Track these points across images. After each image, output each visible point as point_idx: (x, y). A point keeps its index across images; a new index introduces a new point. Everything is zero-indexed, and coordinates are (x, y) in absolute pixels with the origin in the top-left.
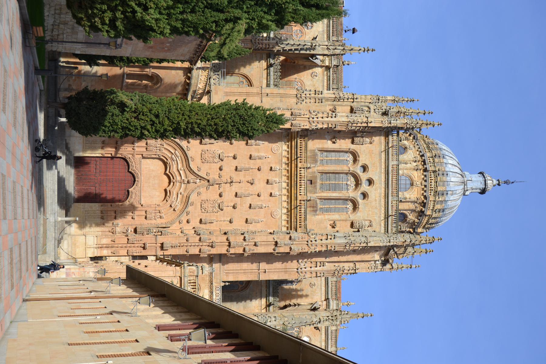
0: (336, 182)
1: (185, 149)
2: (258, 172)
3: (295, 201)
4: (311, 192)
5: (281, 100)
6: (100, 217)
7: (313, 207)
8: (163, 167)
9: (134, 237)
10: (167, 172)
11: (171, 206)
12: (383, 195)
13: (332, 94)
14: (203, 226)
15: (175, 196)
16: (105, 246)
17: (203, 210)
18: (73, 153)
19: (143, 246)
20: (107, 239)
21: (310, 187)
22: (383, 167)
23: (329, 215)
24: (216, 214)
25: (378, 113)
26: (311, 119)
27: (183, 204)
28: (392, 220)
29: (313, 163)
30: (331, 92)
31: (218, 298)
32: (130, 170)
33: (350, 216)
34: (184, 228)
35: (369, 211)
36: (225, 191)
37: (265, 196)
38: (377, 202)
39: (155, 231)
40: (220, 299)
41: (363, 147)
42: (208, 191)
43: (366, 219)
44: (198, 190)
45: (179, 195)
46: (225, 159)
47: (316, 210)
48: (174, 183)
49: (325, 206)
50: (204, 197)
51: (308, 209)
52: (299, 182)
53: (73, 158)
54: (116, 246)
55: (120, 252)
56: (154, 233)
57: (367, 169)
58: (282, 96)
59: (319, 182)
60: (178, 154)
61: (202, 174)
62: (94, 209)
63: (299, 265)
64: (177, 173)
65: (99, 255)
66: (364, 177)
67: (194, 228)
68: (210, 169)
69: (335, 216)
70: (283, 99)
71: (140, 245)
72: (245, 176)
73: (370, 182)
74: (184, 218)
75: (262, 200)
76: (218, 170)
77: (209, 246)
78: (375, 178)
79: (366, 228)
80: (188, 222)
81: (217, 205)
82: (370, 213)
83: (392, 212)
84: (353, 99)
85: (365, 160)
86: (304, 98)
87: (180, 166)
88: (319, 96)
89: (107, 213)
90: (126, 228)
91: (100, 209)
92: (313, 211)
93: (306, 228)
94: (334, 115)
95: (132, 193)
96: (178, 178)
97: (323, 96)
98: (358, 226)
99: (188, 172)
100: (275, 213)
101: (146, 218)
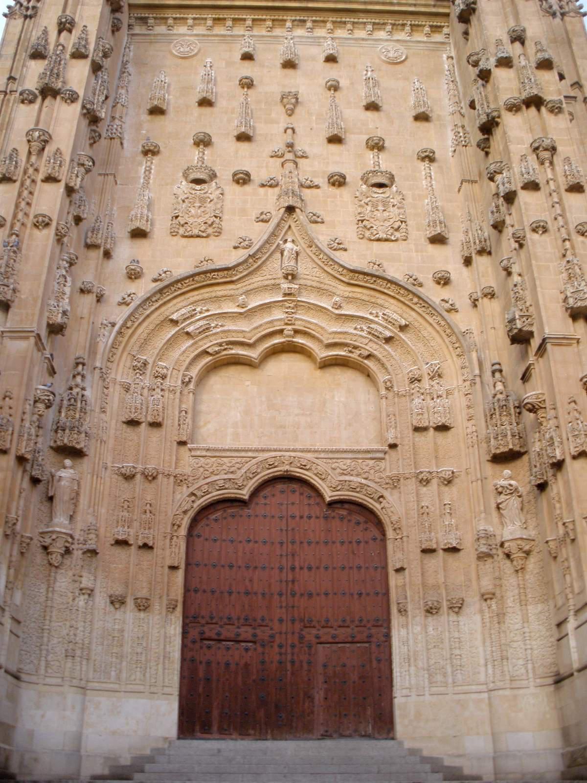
6: (453, 617)
8: (232, 372)
10: (254, 354)
11: (388, 340)
14: (456, 237)
15: (349, 328)
17: (398, 235)
24: (409, 200)
27: (381, 299)
32: (245, 494)
39: (500, 386)
42: (326, 219)
45: (343, 312)
48: (297, 332)
50: (348, 233)
61: (258, 233)
64: (259, 321)
68: (243, 212)
74: (434, 294)
75: (352, 84)
76: (247, 188)
81: (379, 194)
87: (230, 308)
89: (436, 587)
91: (420, 618)
96: (278, 314)
99: (256, 280)
101: (443, 428)
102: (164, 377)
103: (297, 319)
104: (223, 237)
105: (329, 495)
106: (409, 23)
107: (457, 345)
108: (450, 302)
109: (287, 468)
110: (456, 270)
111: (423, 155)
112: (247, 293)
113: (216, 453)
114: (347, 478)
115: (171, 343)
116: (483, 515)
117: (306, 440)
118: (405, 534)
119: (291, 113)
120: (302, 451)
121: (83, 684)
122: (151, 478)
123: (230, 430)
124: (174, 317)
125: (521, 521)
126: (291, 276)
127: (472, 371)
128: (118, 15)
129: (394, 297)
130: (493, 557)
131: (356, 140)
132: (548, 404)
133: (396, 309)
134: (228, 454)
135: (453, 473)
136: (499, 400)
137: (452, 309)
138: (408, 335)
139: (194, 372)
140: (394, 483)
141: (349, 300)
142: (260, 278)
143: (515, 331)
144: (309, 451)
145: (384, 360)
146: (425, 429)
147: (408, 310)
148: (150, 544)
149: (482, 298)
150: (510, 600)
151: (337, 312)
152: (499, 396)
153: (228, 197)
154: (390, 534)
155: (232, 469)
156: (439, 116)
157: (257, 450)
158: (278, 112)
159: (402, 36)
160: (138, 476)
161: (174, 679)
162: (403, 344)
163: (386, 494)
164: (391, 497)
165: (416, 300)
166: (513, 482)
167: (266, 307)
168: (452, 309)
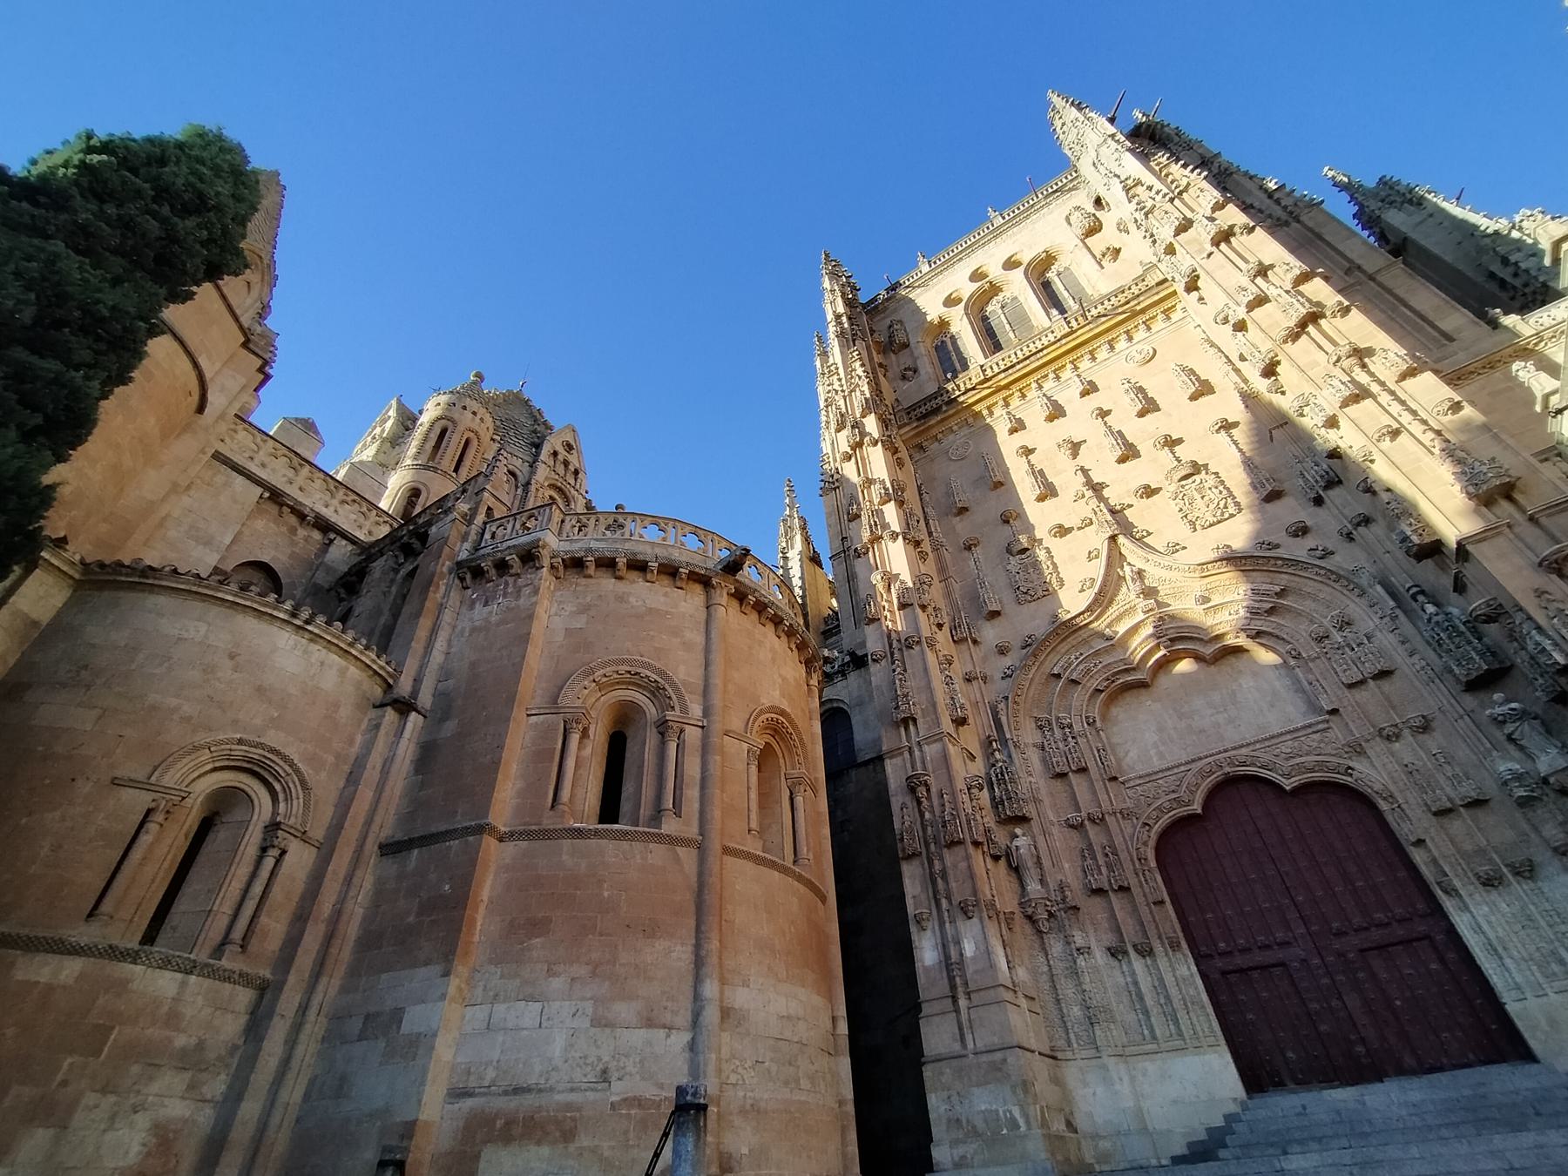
8: (1129, 698)
11: (1271, 611)
18: (1233, 1108)
32: (1197, 807)
37: (1094, 401)
39: (1430, 608)
74: (1298, 549)
100: (1138, 357)
101: (1384, 674)
102: (1070, 726)
103: (1166, 629)
105: (1288, 784)
106: (1140, 322)
107: (1351, 587)
108: (1320, 548)
109: (1227, 769)
110: (1307, 515)
111: (1217, 427)
113: (1149, 777)
114: (1298, 760)
116: (1495, 753)
117: (1232, 736)
118: (1401, 801)
120: (1234, 748)
121: (1120, 1050)
122: (1098, 820)
123: (1153, 752)
125: (1556, 747)
128: (899, 455)
129: (1253, 570)
130: (1541, 800)
132: (1508, 607)
133: (1263, 580)
134: (1161, 775)
135: (1423, 717)
136: (1437, 623)
137: (1327, 553)
138: (1290, 598)
139: (1096, 713)
140: (1358, 750)
142: (1115, 608)
143: (1415, 548)
144: (1242, 746)
145: (1276, 632)
146: (1362, 682)
147: (1277, 575)
148: (1126, 884)
149: (1355, 529)
152: (1435, 619)
154: (1384, 806)
155: (1173, 788)
157: (1187, 763)
160: (1086, 822)
162: (1288, 609)
164: (1359, 765)
165: (1280, 562)
166: (1513, 705)
168: (1327, 553)
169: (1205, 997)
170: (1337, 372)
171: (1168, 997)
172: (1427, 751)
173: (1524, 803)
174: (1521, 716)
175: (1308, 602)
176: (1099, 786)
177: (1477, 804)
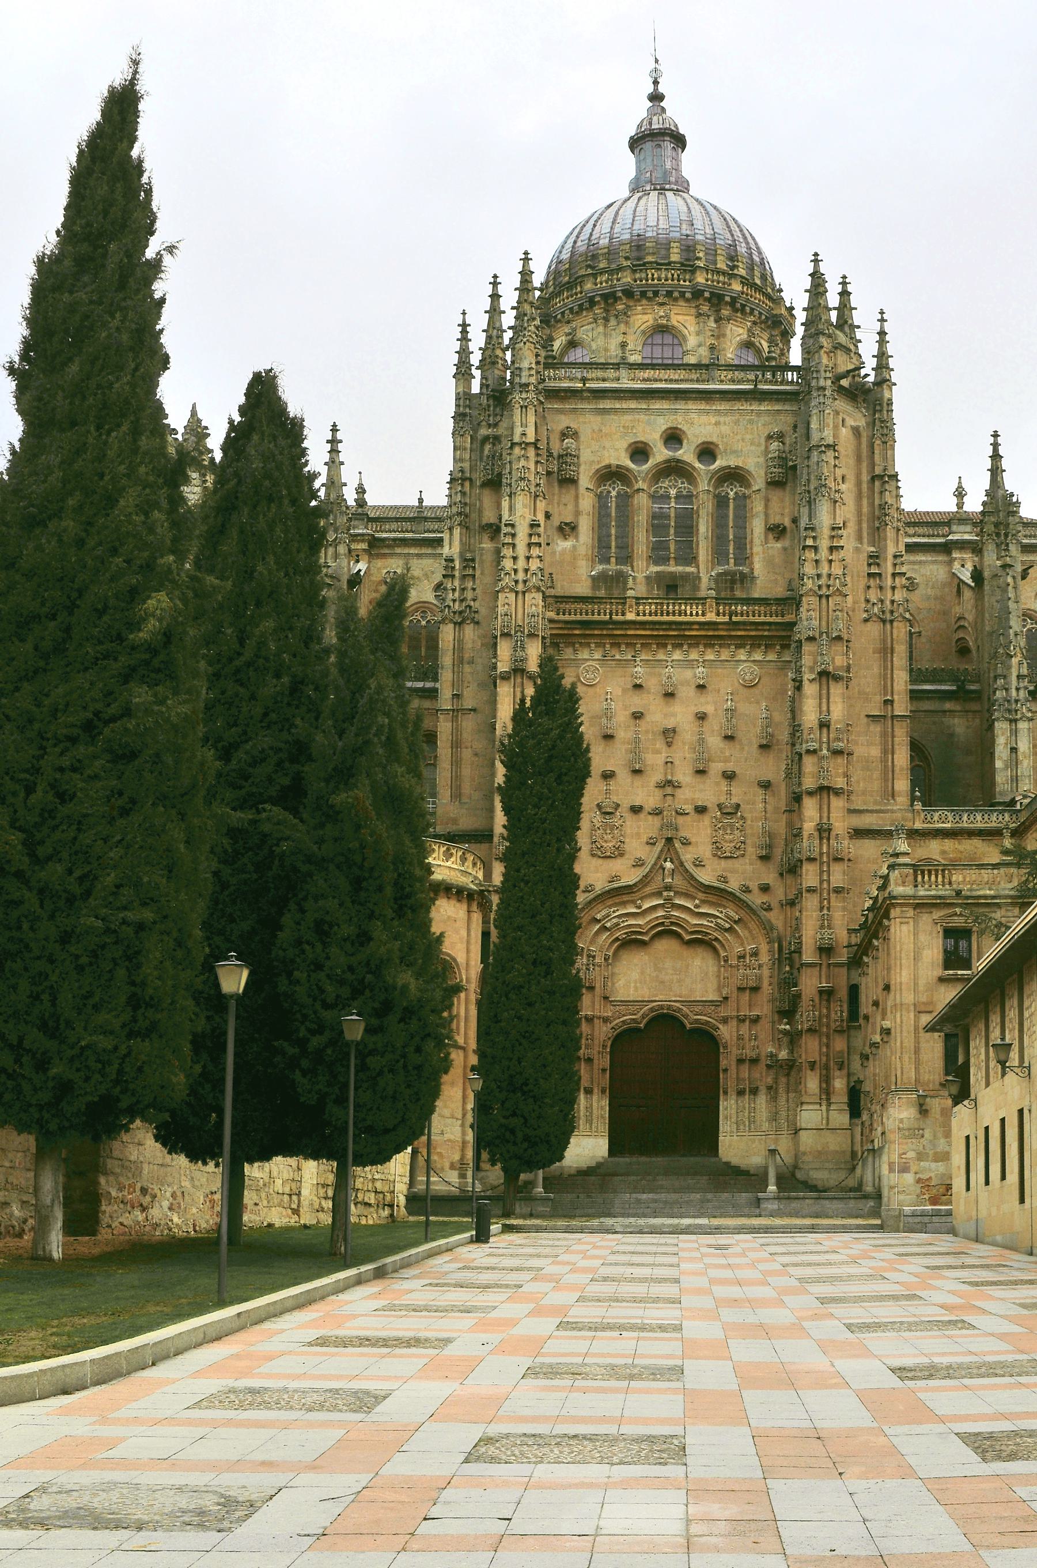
0: (673, 524)
1: (591, 896)
2: (648, 718)
3: (720, 627)
4: (696, 588)
5: (468, 663)
7: (733, 582)
9: (804, 1017)
10: (646, 938)
11: (726, 930)
12: (703, 406)
13: (451, 534)
14: (778, 852)
16: (824, 1085)
18: (601, 1160)
19: (825, 997)
20: (809, 1079)
21: (684, 591)
22: (633, 404)
23: (752, 542)
24: (749, 822)
25: (499, 418)
26: (520, 587)
27: (724, 902)
28: (766, 382)
29: (625, 583)
30: (446, 536)
31: (950, 818)
33: (756, 488)
34: (783, 898)
35: (743, 440)
36: (693, 799)
38: (722, 419)
39: (788, 968)
40: (953, 811)
41: (586, 455)
42: (693, 840)
43: (763, 448)
44: (689, 866)
46: (615, 799)
47: (743, 577)
48: (672, 923)
49: (731, 551)
51: (738, 594)
52: (671, 618)
53: (612, 1159)
54: (824, 1059)
55: (838, 1049)
56: (795, 972)
57: (640, 445)
58: (459, 661)
59: (673, 568)
60: (603, 913)
61: (650, 855)
62: (734, 1112)
63: (874, 619)
65: (845, 1099)
66: (661, 454)
67: (781, 875)
68: (638, 835)
69: (757, 527)
70: (466, 656)
71: (824, 1003)
72: (658, 752)
73: (673, 438)
74: (757, 899)
75: (716, 710)
76: (642, 815)
77: (828, 839)
78: (662, 424)
79: (787, 449)
80: (765, 889)
82: (748, 437)
83: (748, 381)
84: (464, 479)
85: (617, 450)
86: (464, 604)
88: (457, 567)
90: (781, 1036)
92: (742, 582)
93: (787, 599)
94: (509, 529)
95: (697, 1021)
97: (456, 557)
98: (780, 470)
99: (648, 890)
101: (755, 989)
102: (594, 957)
104: (627, 856)
105: (688, 1026)
112: (642, 899)
115: (597, 933)
119: (669, 744)
123: (632, 985)
124: (598, 916)
126: (668, 888)
127: (774, 955)
131: (716, 768)
140: (725, 1021)
141: (703, 902)
150: (781, 1090)
151: (696, 910)
153: (628, 823)
156: (778, 740)
158: (660, 744)
159: (758, 656)
161: (604, 1127)
163: (721, 1026)
167: (654, 908)
168: (769, 909)
169: (607, 1115)
170: (816, 834)
171: (591, 1113)
172: (750, 1031)
173: (768, 1067)
174: (785, 1033)
175: (746, 932)
176: (597, 999)
177: (754, 1061)
